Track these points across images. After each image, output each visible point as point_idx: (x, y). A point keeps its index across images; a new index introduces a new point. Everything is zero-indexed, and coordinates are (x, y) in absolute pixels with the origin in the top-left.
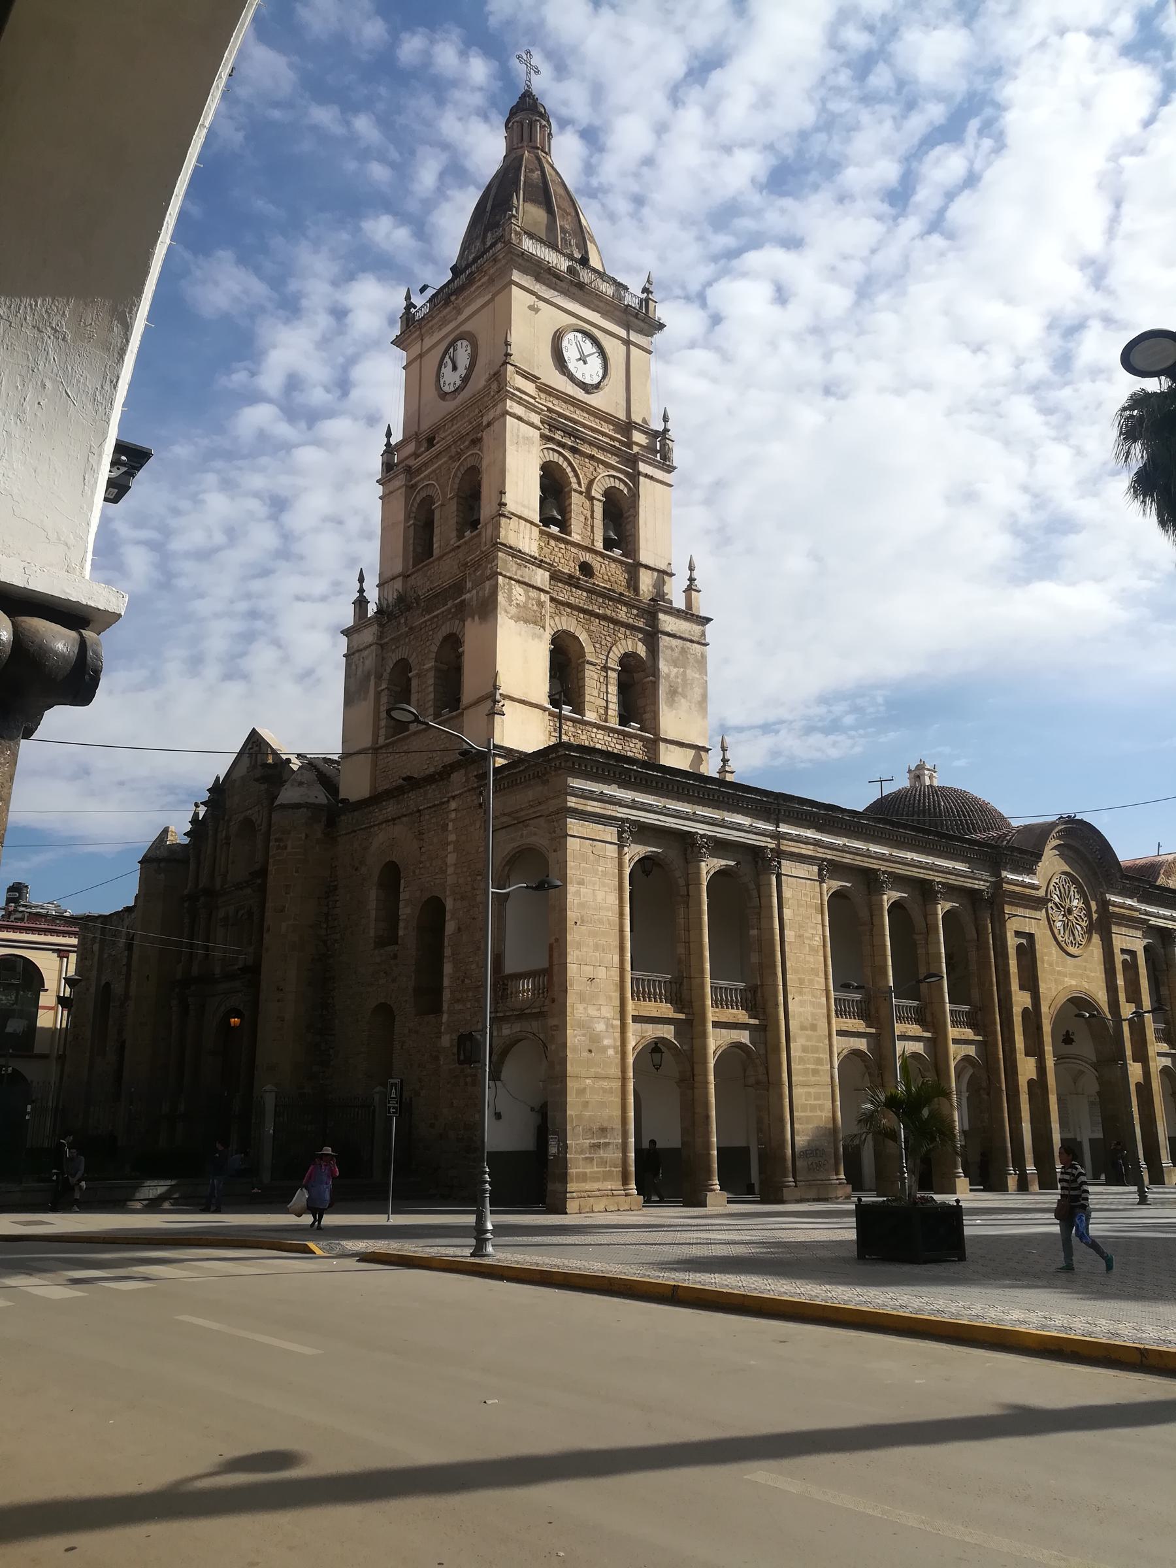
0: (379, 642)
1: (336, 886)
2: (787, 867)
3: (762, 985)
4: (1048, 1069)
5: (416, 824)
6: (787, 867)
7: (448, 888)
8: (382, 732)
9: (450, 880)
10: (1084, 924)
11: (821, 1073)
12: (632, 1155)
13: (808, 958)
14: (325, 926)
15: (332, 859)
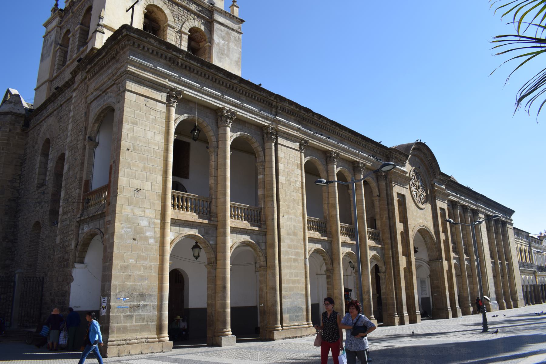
0: (59, 25)
1: (26, 159)
2: (280, 140)
3: (265, 208)
4: (412, 262)
5: (59, 114)
6: (280, 140)
7: (67, 145)
8: (55, 71)
9: (68, 140)
10: (425, 195)
11: (299, 261)
12: (166, 313)
13: (292, 193)
14: (18, 181)
15: (26, 144)
